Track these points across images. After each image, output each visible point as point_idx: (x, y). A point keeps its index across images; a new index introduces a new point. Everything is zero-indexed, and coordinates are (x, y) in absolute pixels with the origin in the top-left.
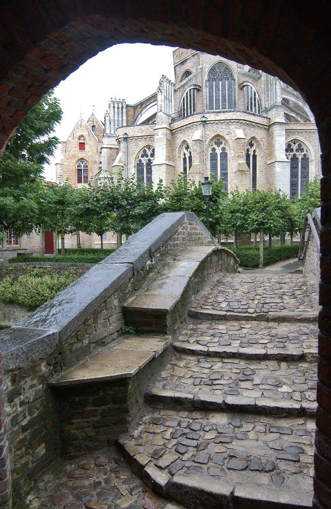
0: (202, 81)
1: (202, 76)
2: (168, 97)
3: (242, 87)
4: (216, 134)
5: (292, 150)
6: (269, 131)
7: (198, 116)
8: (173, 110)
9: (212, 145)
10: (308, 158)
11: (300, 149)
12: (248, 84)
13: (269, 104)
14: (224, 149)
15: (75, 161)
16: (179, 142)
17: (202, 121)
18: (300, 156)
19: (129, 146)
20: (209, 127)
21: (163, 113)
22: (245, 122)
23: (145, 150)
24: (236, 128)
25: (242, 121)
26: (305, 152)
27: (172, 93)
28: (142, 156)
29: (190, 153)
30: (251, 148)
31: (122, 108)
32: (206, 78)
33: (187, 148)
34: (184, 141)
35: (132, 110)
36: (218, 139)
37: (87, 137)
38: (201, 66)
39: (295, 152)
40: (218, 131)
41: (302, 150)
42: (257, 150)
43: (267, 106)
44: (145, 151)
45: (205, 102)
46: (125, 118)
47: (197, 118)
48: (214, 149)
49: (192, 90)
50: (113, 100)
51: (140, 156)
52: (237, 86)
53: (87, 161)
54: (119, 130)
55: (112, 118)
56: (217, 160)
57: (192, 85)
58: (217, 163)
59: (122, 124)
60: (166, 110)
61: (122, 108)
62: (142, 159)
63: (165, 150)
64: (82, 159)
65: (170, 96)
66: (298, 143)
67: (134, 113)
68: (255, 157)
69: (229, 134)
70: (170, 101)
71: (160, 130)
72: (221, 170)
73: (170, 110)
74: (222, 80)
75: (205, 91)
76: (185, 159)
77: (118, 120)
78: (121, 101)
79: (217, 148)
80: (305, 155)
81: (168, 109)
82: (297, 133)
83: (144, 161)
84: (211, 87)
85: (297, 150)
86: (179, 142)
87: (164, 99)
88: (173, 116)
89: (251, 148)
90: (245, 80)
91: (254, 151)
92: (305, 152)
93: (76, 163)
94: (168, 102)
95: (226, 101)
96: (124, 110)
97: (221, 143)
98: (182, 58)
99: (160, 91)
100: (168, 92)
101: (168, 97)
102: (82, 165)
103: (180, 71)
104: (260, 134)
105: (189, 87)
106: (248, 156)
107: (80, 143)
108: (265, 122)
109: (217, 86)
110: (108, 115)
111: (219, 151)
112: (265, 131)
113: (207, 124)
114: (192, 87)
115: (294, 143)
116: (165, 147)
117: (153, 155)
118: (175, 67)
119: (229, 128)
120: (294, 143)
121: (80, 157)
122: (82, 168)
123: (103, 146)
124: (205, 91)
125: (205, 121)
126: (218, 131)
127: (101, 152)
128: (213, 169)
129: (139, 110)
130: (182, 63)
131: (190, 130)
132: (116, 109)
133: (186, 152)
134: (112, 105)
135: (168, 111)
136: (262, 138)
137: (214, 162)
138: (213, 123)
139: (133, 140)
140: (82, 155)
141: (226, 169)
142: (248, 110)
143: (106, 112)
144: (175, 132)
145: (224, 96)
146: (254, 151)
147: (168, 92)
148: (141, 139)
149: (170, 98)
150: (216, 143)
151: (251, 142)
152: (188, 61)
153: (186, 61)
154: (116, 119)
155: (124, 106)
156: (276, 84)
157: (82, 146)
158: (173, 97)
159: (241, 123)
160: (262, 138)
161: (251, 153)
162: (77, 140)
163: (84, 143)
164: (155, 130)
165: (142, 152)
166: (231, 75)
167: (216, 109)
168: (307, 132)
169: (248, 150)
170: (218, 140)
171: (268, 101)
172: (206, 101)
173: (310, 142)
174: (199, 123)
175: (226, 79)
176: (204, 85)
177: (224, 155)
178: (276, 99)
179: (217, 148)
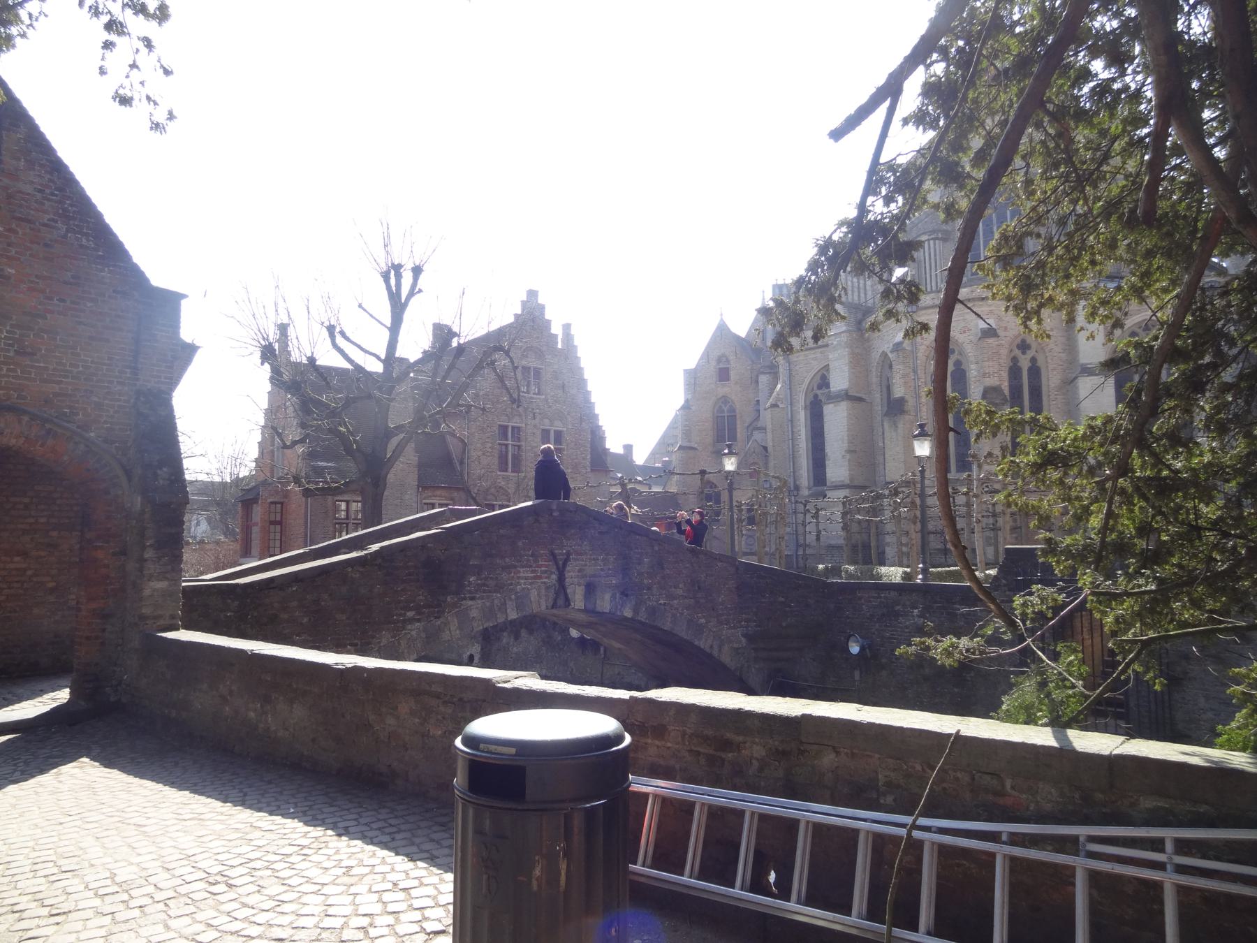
16: (876, 356)
28: (820, 387)
30: (1024, 353)
33: (891, 367)
34: (884, 355)
50: (781, 282)
62: (819, 392)
63: (847, 374)
68: (1035, 371)
81: (856, 294)
86: (876, 356)
88: (870, 303)
89: (1024, 353)
91: (1033, 360)
106: (1015, 371)
135: (856, 298)
146: (1033, 360)
165: (818, 377)
169: (1015, 360)
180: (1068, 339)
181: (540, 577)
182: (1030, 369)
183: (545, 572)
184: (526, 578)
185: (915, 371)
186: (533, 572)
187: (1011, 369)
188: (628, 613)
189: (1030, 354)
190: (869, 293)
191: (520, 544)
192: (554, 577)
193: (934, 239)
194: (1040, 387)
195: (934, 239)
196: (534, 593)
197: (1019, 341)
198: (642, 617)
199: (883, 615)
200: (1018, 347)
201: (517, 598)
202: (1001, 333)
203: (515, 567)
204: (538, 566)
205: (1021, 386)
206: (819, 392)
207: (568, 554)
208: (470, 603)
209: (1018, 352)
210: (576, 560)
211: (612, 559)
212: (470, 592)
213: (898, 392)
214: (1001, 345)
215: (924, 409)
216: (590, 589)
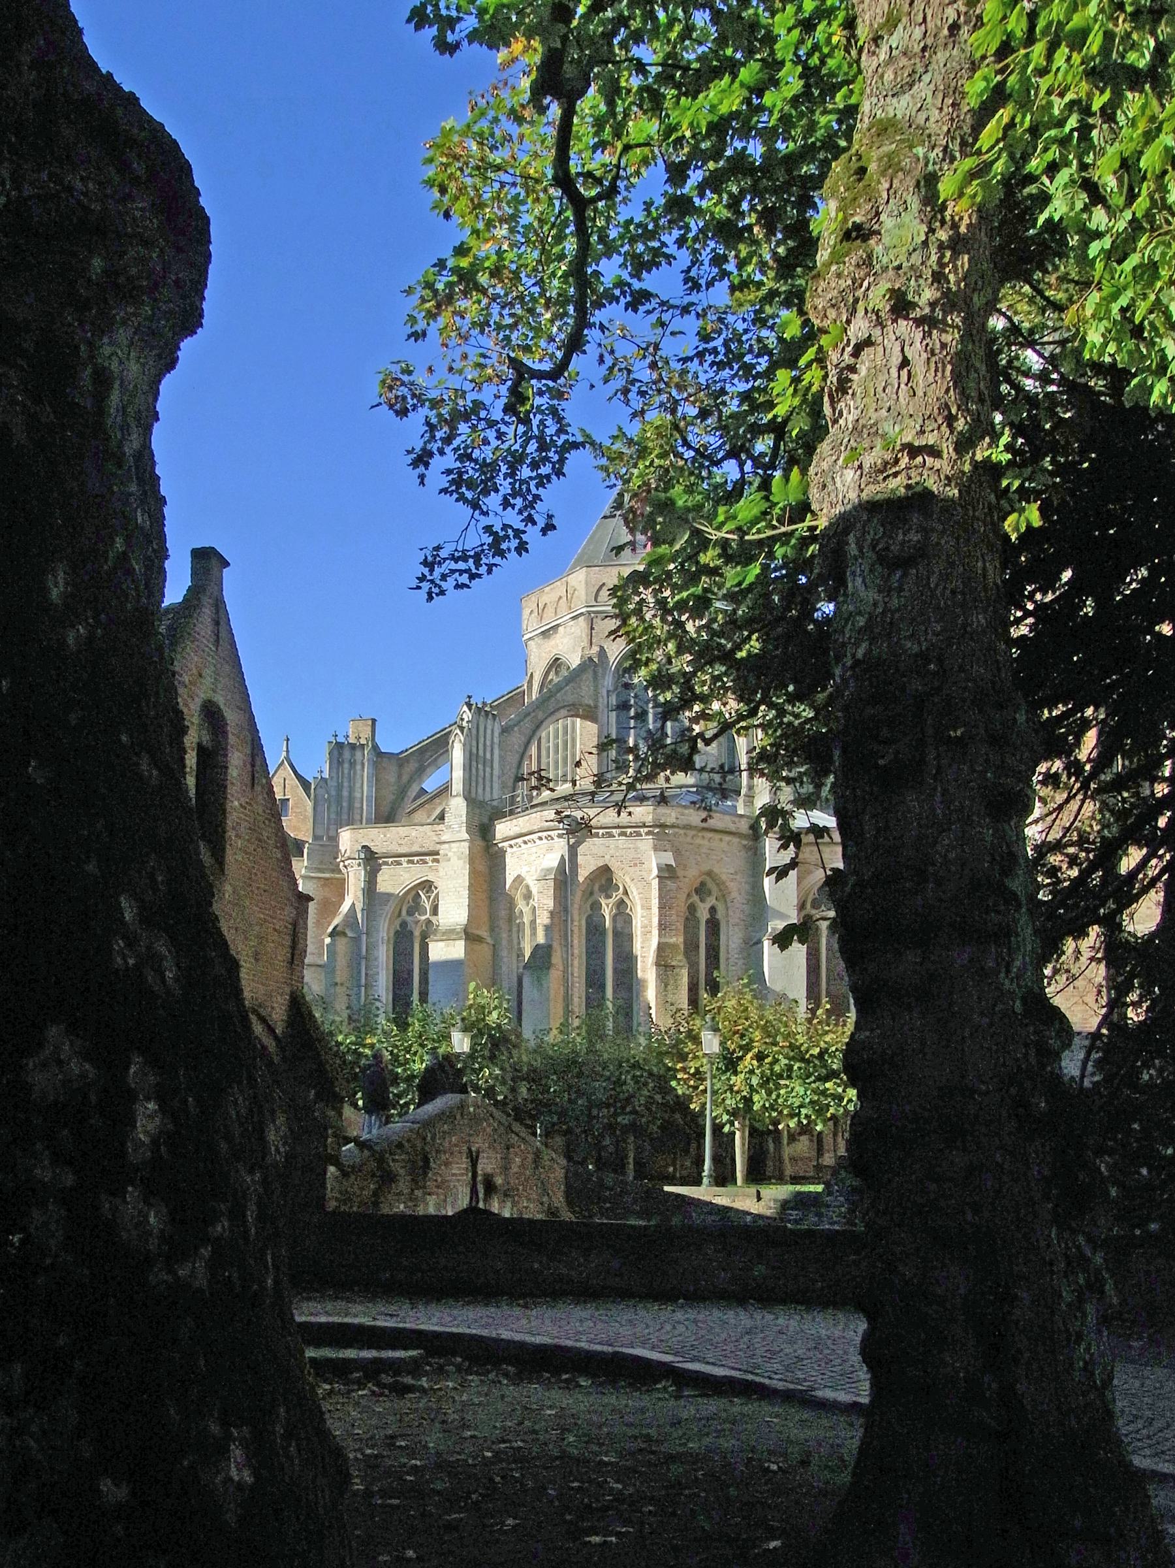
2: (481, 753)
14: (621, 904)
27: (496, 740)
40: (607, 857)
50: (341, 739)
51: (404, 912)
60: (473, 790)
65: (489, 749)
68: (714, 926)
69: (635, 865)
70: (488, 764)
73: (488, 789)
89: (702, 900)
91: (713, 910)
103: (540, 658)
117: (435, 911)
119: (636, 849)
129: (413, 765)
135: (480, 791)
146: (713, 910)
147: (481, 740)
149: (488, 756)
158: (496, 752)
169: (692, 909)
180: (753, 888)
189: (711, 901)
190: (496, 786)
200: (697, 891)
209: (696, 898)
215: (576, 963)
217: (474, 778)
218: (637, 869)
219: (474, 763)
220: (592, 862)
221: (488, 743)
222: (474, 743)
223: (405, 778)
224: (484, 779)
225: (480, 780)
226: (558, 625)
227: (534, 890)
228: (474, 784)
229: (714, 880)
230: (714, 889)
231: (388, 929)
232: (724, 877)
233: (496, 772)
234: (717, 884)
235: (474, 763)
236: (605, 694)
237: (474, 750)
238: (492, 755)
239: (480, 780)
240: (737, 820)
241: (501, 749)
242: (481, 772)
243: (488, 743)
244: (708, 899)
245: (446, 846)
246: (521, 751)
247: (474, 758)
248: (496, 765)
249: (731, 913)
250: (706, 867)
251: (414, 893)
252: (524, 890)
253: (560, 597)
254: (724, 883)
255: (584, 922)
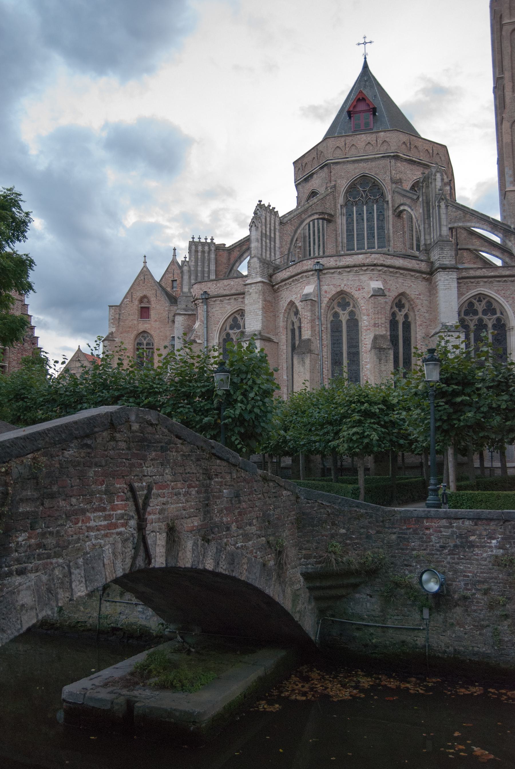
0: (335, 206)
1: (335, 198)
2: (268, 233)
3: (399, 214)
4: (339, 289)
5: (476, 313)
6: (431, 283)
7: (310, 262)
8: (278, 253)
9: (333, 308)
10: (504, 325)
11: (491, 308)
12: (406, 208)
13: (431, 239)
14: (352, 314)
15: (132, 336)
16: (284, 304)
17: (316, 270)
18: (490, 321)
19: (209, 309)
20: (327, 279)
21: (259, 259)
22: (386, 269)
23: (235, 317)
24: (371, 279)
25: (380, 268)
26: (498, 315)
27: (277, 227)
28: (232, 328)
29: (300, 320)
30: (400, 311)
31: (209, 252)
32: (341, 200)
33: (297, 313)
35: (225, 254)
36: (343, 299)
37: (153, 299)
38: (333, 183)
39: (480, 315)
40: (343, 285)
41: (494, 312)
42: (411, 314)
43: (429, 242)
44: (235, 320)
45: (340, 239)
46: (213, 267)
47: (309, 264)
48: (336, 315)
49: (316, 221)
50: (196, 240)
51: (228, 328)
52: (391, 212)
53: (151, 336)
54: (195, 286)
55: (192, 269)
56: (341, 331)
57: (316, 213)
58: (341, 336)
59: (209, 276)
60: (264, 254)
61: (209, 252)
62: (231, 332)
63: (260, 317)
64: (144, 332)
65: (273, 232)
66: (486, 300)
67: (229, 259)
68: (407, 326)
69: (359, 290)
70: (273, 240)
71: (253, 285)
72: (349, 347)
73: (273, 254)
74: (367, 203)
75: (341, 221)
76: (293, 331)
77: (203, 272)
78: (209, 241)
79: (341, 312)
80: (499, 320)
81: (268, 252)
82: (482, 284)
83: (234, 334)
84: (349, 215)
85: (485, 312)
86: (284, 304)
87: (259, 238)
88: (278, 262)
89: (400, 311)
90: (402, 202)
91: (406, 316)
92: (498, 315)
93: (135, 339)
94: (268, 241)
95: (374, 237)
96: (213, 256)
97: (348, 304)
98: (308, 171)
99: (254, 225)
100: (268, 226)
101: (268, 233)
102: (145, 342)
104: (414, 288)
105: (310, 216)
106: (393, 324)
107: (142, 308)
108: (423, 266)
109: (360, 214)
110: (186, 263)
111: (344, 317)
112: (425, 283)
113: (325, 274)
114: (316, 216)
115: (480, 301)
116: (260, 312)
118: (297, 186)
119: (359, 280)
120: (480, 301)
121: (141, 330)
122: (145, 347)
123: (178, 312)
124: (341, 221)
125: (320, 270)
126: (343, 285)
127: (173, 322)
128: (336, 345)
129: (236, 253)
130: (307, 180)
131: (299, 285)
132: (200, 254)
133: (295, 320)
134: (193, 247)
135: (268, 256)
136: (420, 295)
137: (337, 334)
138: (333, 273)
139: (218, 302)
140: (143, 326)
141: (357, 346)
142: (413, 249)
143: (184, 259)
144: (278, 288)
145: (371, 228)
146: (406, 316)
147: (268, 226)
148: (229, 299)
149: (272, 235)
150: (339, 305)
151: (400, 301)
152: (315, 176)
153: (311, 176)
154: (199, 269)
155: (213, 249)
156: (439, 206)
157: (144, 312)
158: (277, 234)
159: (380, 271)
160: (420, 295)
161: (400, 319)
162: (136, 303)
163: (148, 308)
164: (245, 285)
165: (230, 320)
166: (382, 195)
167: (358, 249)
168: (499, 281)
169: (394, 314)
170: (343, 299)
171: (430, 234)
172: (343, 238)
173: (504, 297)
174: (311, 273)
175: (373, 202)
176: (339, 211)
177: (354, 323)
178: (440, 230)
179: (341, 312)
181: (116, 526)
182: (404, 323)
183: (122, 516)
184: (98, 529)
185: (319, 319)
186: (106, 518)
187: (391, 321)
188: (209, 565)
189: (404, 312)
190: (278, 253)
191: (91, 474)
192: (133, 523)
193: (318, 219)
194: (410, 337)
195: (323, 219)
196: (108, 549)
197: (397, 301)
198: (223, 568)
199: (456, 546)
201: (86, 563)
202: (387, 293)
203: (83, 511)
204: (113, 509)
205: (398, 336)
206: (231, 332)
207: (150, 488)
208: (18, 580)
209: (396, 309)
210: (159, 495)
211: (193, 491)
212: (18, 561)
213: (306, 334)
214: (386, 302)
215: (325, 350)
216: (172, 533)
217: (264, 247)
218: (361, 291)
219: (264, 239)
220: (334, 289)
221: (272, 228)
222: (264, 227)
223: (232, 261)
224: (270, 248)
225: (268, 249)
226: (313, 174)
227: (299, 308)
228: (264, 251)
229: (407, 299)
230: (407, 306)
231: (219, 338)
232: (413, 297)
233: (277, 245)
234: (409, 301)
235: (264, 239)
236: (339, 207)
237: (264, 232)
238: (275, 234)
239: (268, 249)
240: (419, 262)
241: (280, 232)
242: (268, 244)
243: (272, 228)
244: (403, 310)
245: (249, 286)
246: (292, 234)
247: (264, 236)
248: (277, 241)
249: (417, 318)
250: (401, 291)
251: (233, 316)
252: (295, 310)
253: (314, 158)
254: (413, 300)
255: (329, 326)
